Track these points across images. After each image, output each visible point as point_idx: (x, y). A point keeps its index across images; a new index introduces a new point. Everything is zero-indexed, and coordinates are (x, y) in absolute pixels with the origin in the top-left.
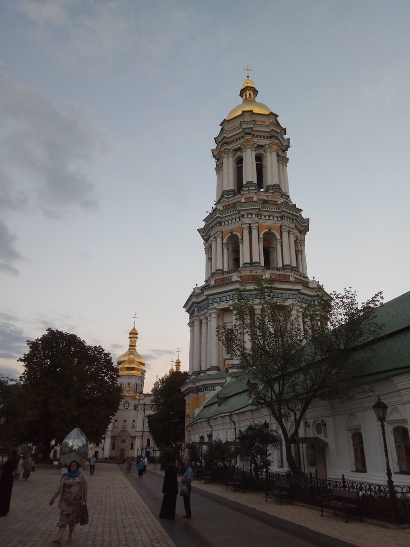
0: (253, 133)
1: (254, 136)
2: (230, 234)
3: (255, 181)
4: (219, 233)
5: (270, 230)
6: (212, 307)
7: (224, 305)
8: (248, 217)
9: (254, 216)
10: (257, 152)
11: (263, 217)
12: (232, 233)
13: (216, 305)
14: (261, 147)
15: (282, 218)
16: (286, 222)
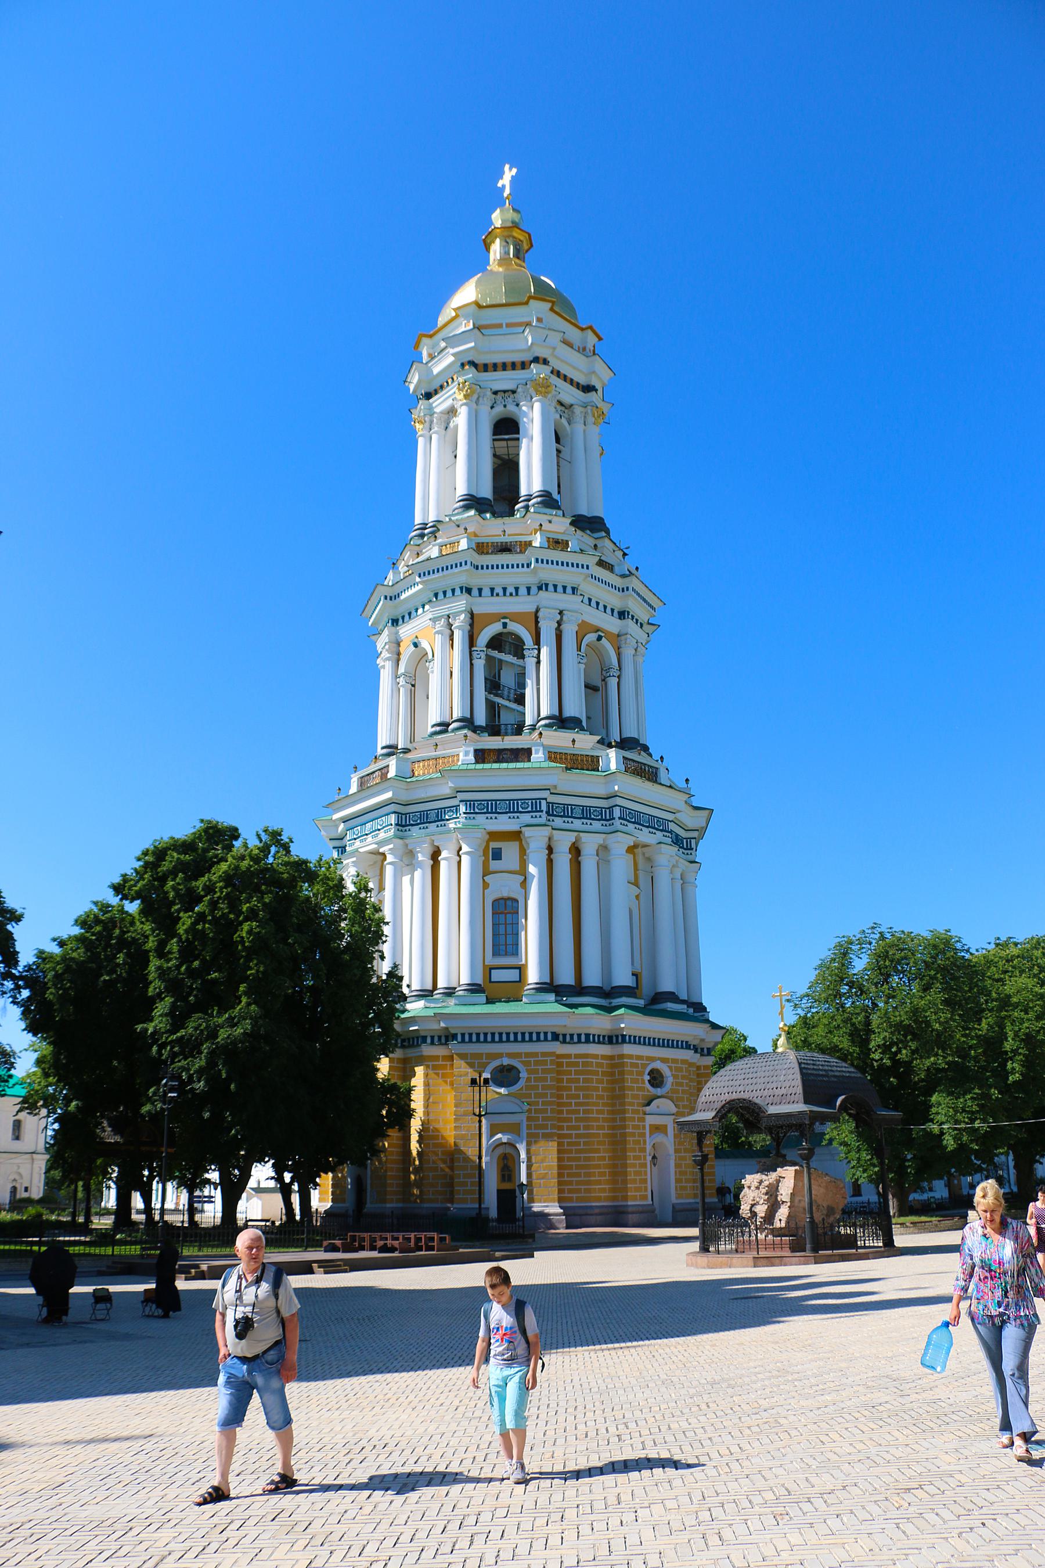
0: (480, 360)
1: (485, 368)
2: (412, 648)
3: (486, 491)
4: (387, 647)
5: (505, 625)
6: (354, 847)
7: (367, 845)
8: (453, 595)
9: (458, 592)
10: (499, 409)
11: (486, 592)
12: (416, 645)
13: (358, 843)
14: (514, 392)
15: (540, 588)
16: (546, 598)
